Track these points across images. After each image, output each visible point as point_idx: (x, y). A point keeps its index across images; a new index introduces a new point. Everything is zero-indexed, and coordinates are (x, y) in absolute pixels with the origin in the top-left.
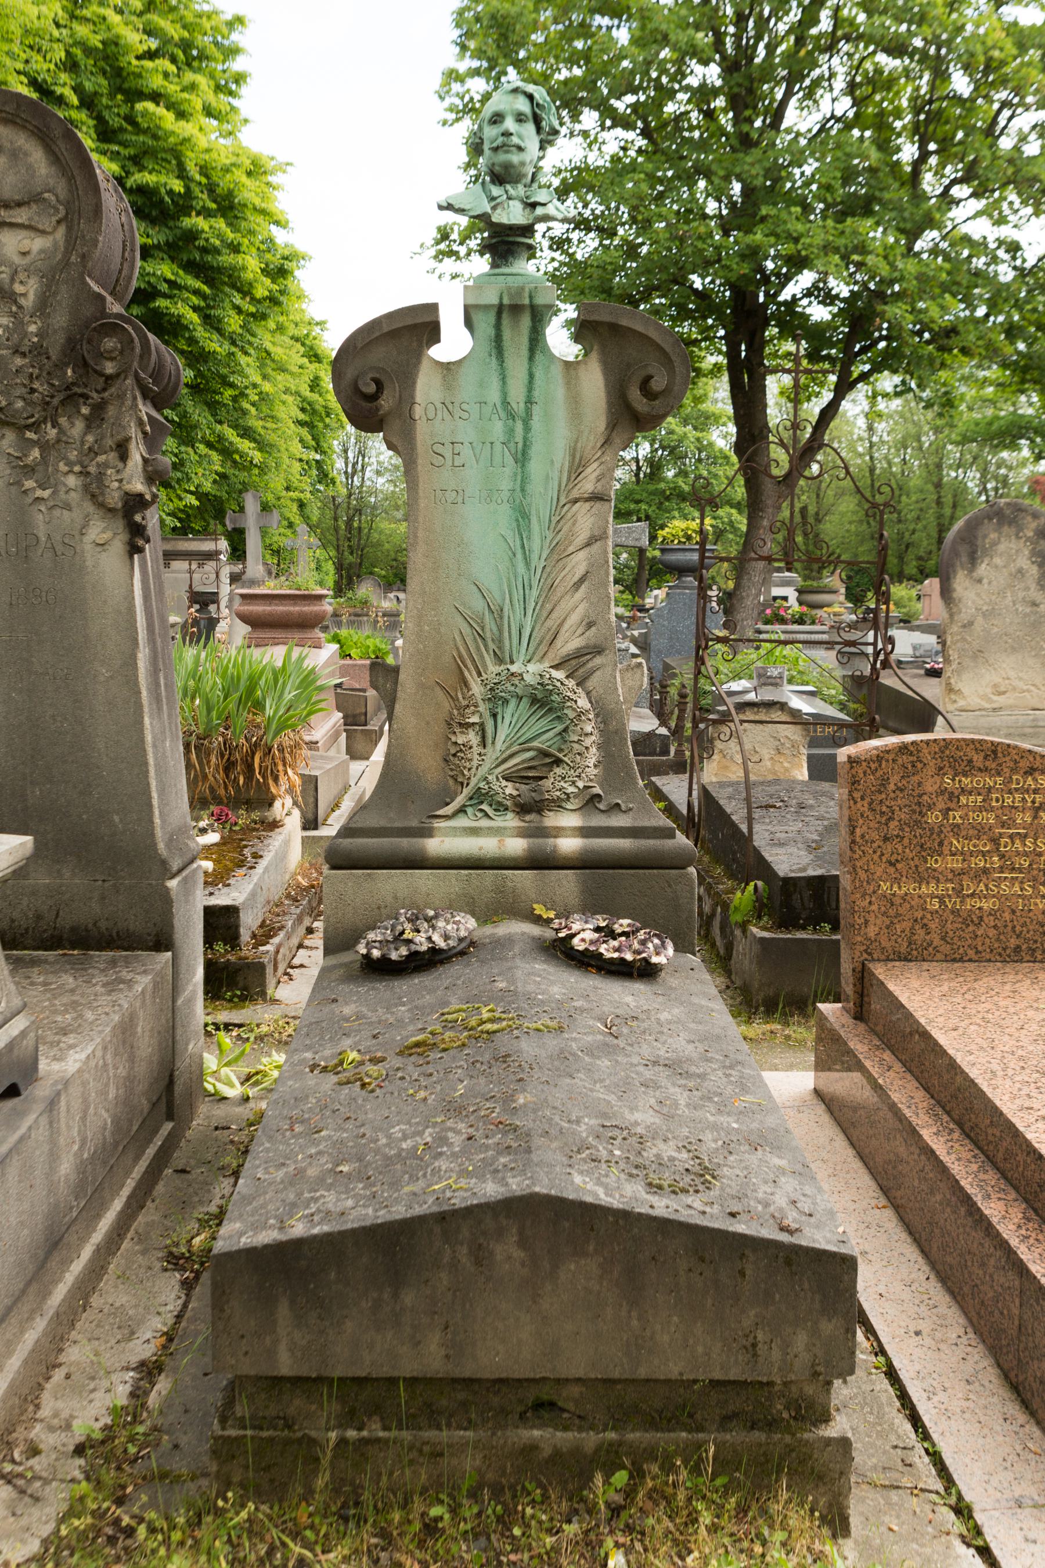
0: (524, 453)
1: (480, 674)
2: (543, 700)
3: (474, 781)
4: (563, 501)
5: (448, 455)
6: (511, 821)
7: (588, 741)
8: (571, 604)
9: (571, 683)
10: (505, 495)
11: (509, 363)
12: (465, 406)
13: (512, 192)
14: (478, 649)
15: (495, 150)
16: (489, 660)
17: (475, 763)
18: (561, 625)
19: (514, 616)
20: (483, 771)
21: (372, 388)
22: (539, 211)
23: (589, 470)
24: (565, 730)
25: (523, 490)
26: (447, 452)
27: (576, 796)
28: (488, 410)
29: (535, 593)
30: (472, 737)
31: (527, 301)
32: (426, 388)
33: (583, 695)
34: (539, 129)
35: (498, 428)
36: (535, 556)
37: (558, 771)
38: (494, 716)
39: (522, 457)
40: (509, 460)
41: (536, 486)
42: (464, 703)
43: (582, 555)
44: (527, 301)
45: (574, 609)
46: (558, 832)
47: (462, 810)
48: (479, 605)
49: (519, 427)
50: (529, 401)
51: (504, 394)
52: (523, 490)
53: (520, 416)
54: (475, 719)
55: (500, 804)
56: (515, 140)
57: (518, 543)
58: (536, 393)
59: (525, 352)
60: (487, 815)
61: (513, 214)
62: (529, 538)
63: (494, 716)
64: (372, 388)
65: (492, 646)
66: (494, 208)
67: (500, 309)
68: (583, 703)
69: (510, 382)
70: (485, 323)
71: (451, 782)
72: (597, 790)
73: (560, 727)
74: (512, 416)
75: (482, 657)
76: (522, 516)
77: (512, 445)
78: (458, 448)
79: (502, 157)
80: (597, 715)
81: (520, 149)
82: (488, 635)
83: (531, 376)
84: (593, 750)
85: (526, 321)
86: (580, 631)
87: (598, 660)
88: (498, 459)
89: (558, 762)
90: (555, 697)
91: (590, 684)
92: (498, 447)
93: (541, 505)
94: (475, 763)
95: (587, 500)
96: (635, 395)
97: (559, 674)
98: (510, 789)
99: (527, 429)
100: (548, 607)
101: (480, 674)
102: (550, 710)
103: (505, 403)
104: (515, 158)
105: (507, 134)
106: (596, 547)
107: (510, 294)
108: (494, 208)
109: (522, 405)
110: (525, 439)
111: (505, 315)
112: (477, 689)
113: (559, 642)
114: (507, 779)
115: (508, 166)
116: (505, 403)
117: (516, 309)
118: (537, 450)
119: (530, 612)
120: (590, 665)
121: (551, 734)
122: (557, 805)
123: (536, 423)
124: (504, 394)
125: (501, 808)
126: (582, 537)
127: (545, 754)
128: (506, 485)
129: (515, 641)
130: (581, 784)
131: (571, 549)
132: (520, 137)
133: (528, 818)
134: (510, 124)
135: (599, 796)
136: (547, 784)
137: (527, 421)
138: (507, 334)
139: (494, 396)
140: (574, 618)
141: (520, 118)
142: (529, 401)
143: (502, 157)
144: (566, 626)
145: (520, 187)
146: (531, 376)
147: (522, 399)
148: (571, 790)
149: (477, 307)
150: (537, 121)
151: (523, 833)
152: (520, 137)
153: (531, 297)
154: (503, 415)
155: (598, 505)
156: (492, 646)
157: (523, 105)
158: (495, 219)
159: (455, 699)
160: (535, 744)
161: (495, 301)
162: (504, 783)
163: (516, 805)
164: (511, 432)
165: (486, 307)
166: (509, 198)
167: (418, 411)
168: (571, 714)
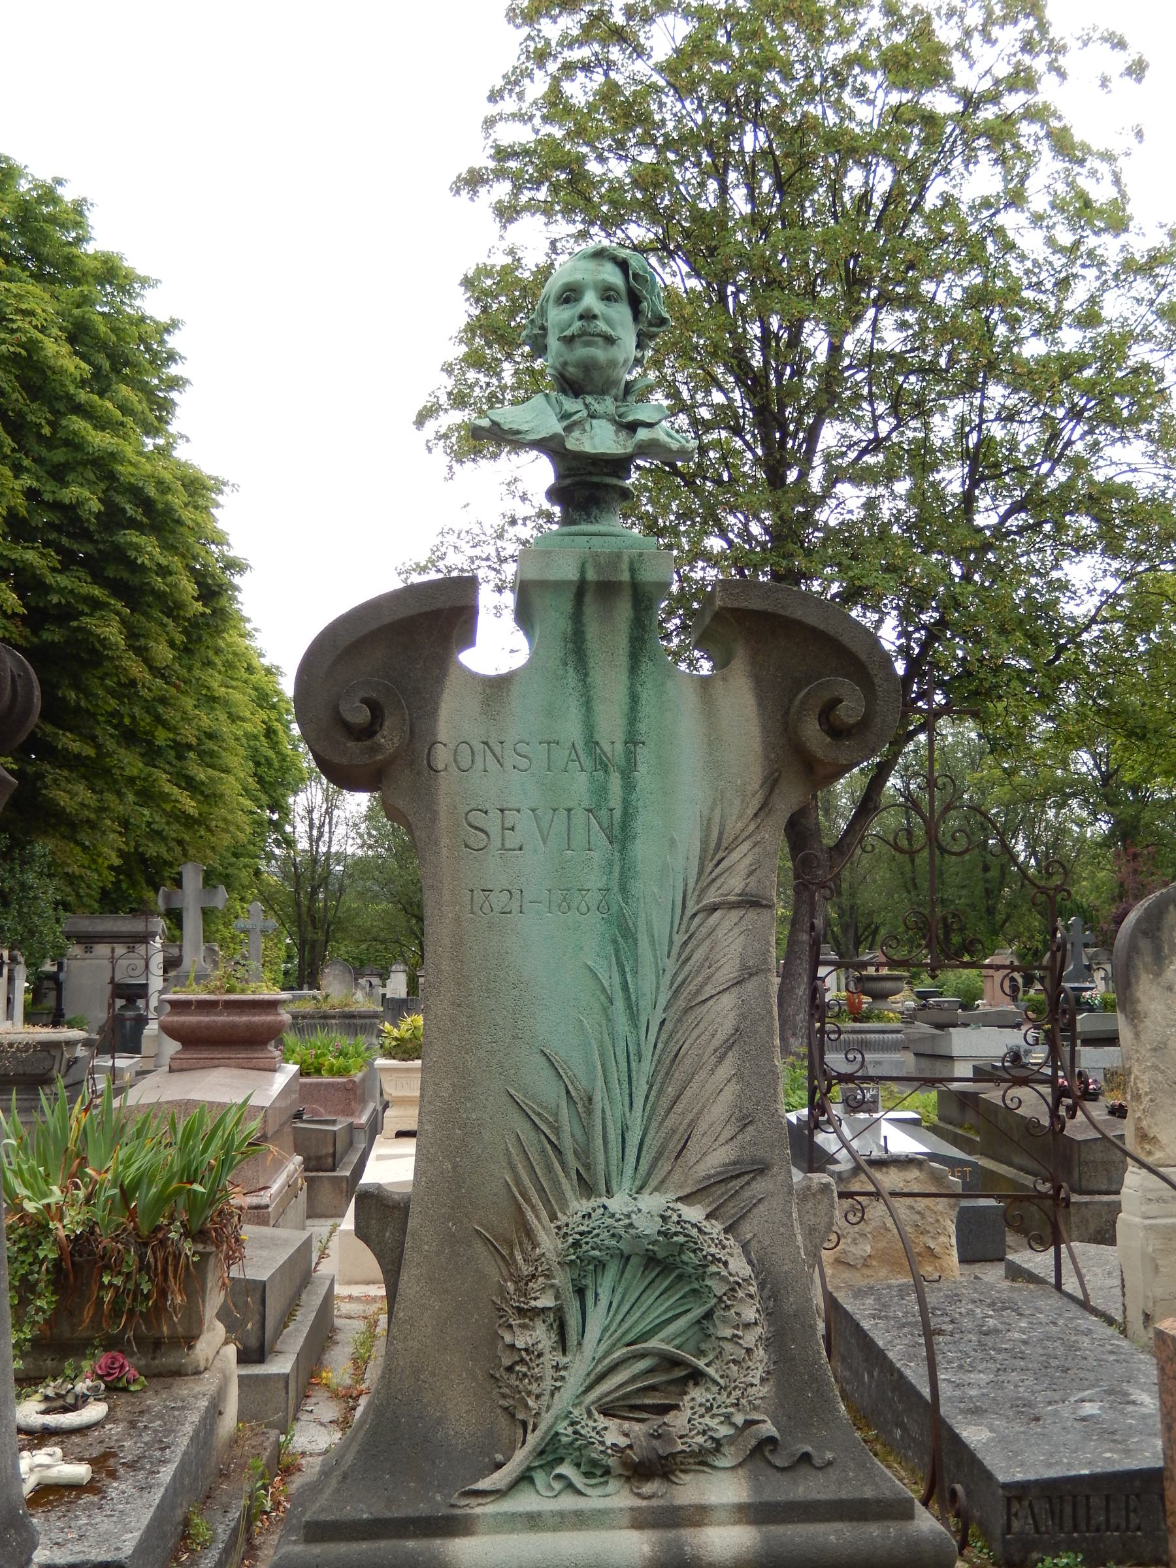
0: (625, 826)
1: (553, 1217)
2: (666, 1263)
3: (546, 1420)
4: (692, 907)
5: (494, 829)
6: (617, 1497)
7: (750, 1338)
8: (710, 1087)
9: (715, 1228)
10: (593, 897)
11: (597, 676)
12: (522, 748)
13: (596, 407)
14: (549, 1168)
15: (569, 341)
16: (568, 1187)
17: (548, 1384)
18: (692, 1125)
19: (610, 1107)
20: (563, 1400)
21: (362, 716)
22: (643, 434)
23: (735, 856)
24: (708, 1315)
25: (623, 890)
26: (492, 824)
27: (731, 1440)
28: (561, 755)
29: (647, 1067)
30: (541, 1335)
31: (625, 577)
32: (454, 720)
33: (738, 1250)
34: (637, 314)
35: (579, 784)
36: (645, 1004)
37: (698, 1394)
38: (580, 1292)
39: (621, 834)
40: (600, 839)
41: (645, 885)
42: (526, 1270)
43: (728, 1000)
44: (625, 577)
45: (716, 1095)
46: (699, 1515)
47: (525, 1478)
48: (548, 1091)
49: (615, 783)
50: (632, 741)
51: (589, 728)
52: (623, 890)
53: (616, 766)
54: (546, 1301)
55: (594, 1463)
56: (602, 326)
57: (617, 979)
58: (642, 727)
59: (623, 660)
60: (570, 1486)
61: (601, 439)
62: (635, 972)
63: (580, 1292)
64: (362, 716)
65: (573, 1163)
66: (569, 429)
67: (581, 590)
68: (739, 1267)
69: (599, 708)
70: (555, 616)
71: (503, 1421)
72: (768, 1429)
73: (698, 1312)
74: (602, 764)
75: (556, 1183)
76: (623, 933)
77: (603, 812)
78: (511, 818)
79: (582, 351)
80: (762, 1286)
81: (610, 340)
82: (567, 1144)
83: (634, 699)
84: (760, 1353)
85: (624, 610)
86: (726, 1135)
87: (760, 1186)
88: (579, 836)
89: (697, 1376)
90: (688, 1256)
91: (747, 1230)
92: (579, 816)
93: (655, 916)
94: (548, 1384)
95: (733, 906)
96: (812, 732)
97: (694, 1213)
98: (614, 1433)
99: (629, 786)
100: (671, 1090)
101: (553, 1217)
102: (680, 1277)
103: (592, 743)
104: (599, 353)
105: (588, 316)
106: (750, 985)
107: (598, 566)
108: (569, 429)
109: (619, 747)
110: (626, 803)
111: (588, 599)
112: (548, 1244)
113: (691, 1154)
114: (606, 1413)
115: (588, 367)
116: (592, 743)
117: (607, 589)
118: (646, 821)
119: (639, 1101)
120: (747, 1193)
121: (682, 1323)
122: (702, 1460)
123: (644, 775)
124: (589, 728)
125: (596, 1471)
126: (728, 970)
127: (670, 1362)
128: (595, 880)
129: (615, 1153)
130: (739, 1419)
131: (709, 991)
132: (608, 322)
133: (648, 1488)
134: (590, 300)
135: (771, 1440)
136: (678, 1421)
137: (628, 772)
138: (592, 630)
139: (571, 729)
140: (719, 1110)
141: (607, 294)
142: (632, 741)
143: (582, 351)
144: (703, 1125)
145: (609, 400)
146: (634, 699)
147: (619, 736)
148: (724, 1431)
149: (543, 585)
150: (634, 301)
151: (640, 1521)
152: (608, 322)
153: (632, 570)
154: (587, 763)
155: (752, 914)
156: (573, 1163)
157: (612, 275)
158: (571, 444)
159: (509, 1262)
160: (654, 1343)
161: (572, 575)
162: (603, 1422)
163: (626, 1464)
164: (601, 792)
165: (557, 586)
166: (593, 416)
167: (442, 756)
168: (719, 1289)
